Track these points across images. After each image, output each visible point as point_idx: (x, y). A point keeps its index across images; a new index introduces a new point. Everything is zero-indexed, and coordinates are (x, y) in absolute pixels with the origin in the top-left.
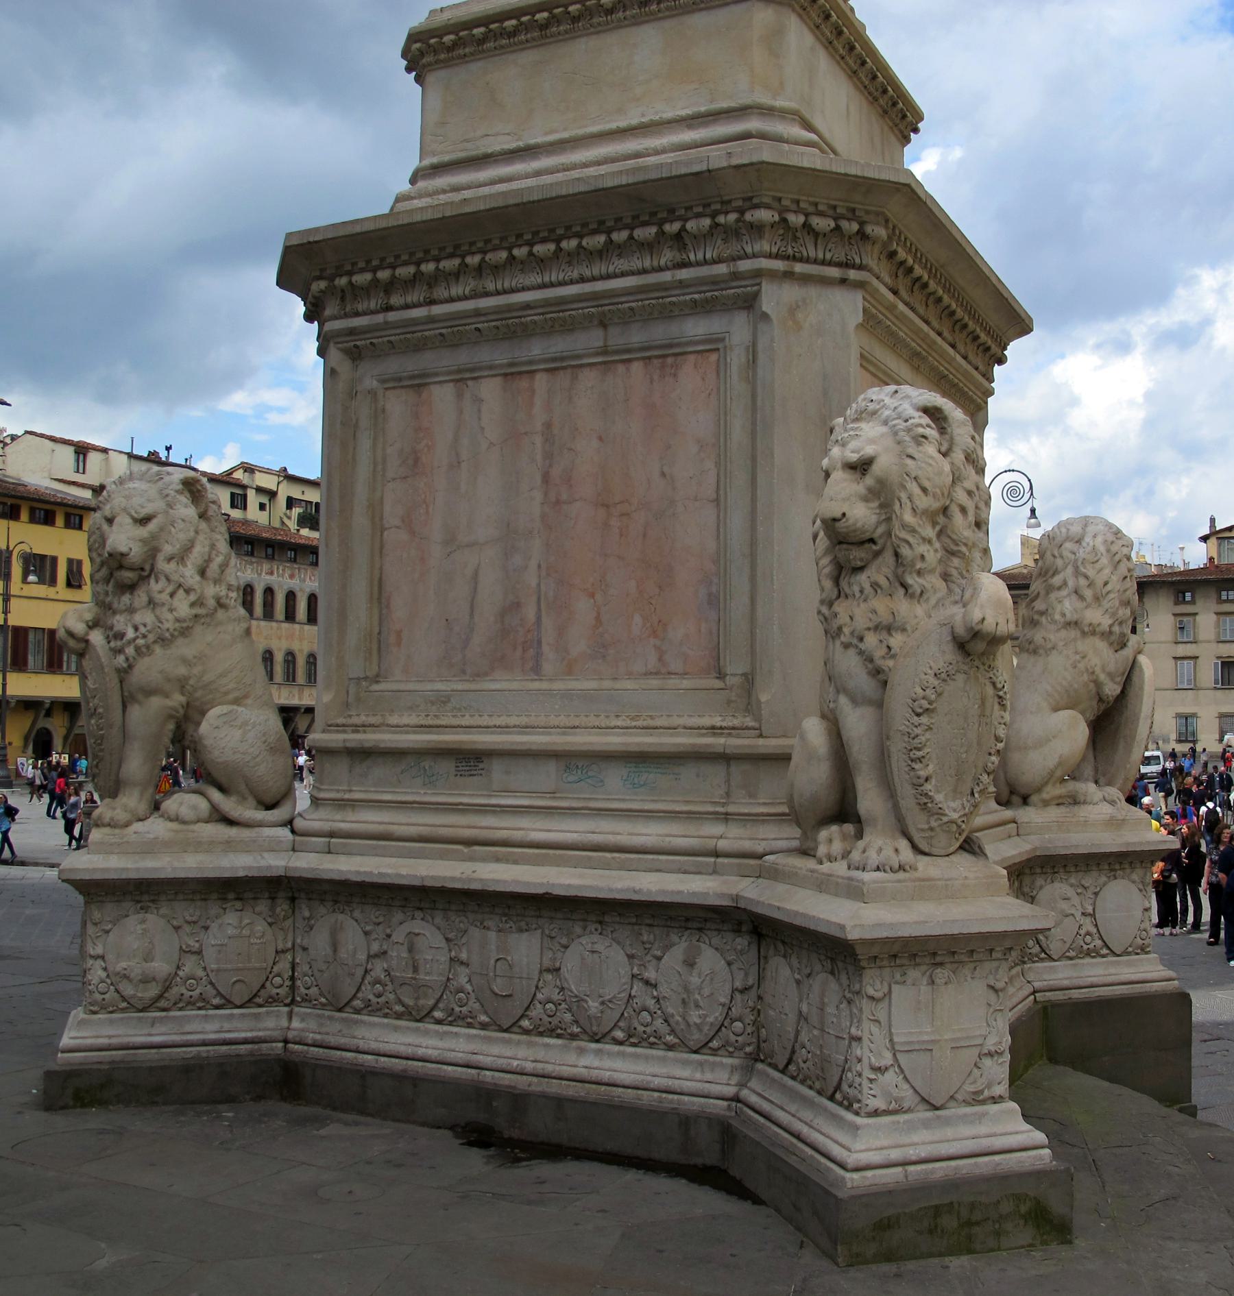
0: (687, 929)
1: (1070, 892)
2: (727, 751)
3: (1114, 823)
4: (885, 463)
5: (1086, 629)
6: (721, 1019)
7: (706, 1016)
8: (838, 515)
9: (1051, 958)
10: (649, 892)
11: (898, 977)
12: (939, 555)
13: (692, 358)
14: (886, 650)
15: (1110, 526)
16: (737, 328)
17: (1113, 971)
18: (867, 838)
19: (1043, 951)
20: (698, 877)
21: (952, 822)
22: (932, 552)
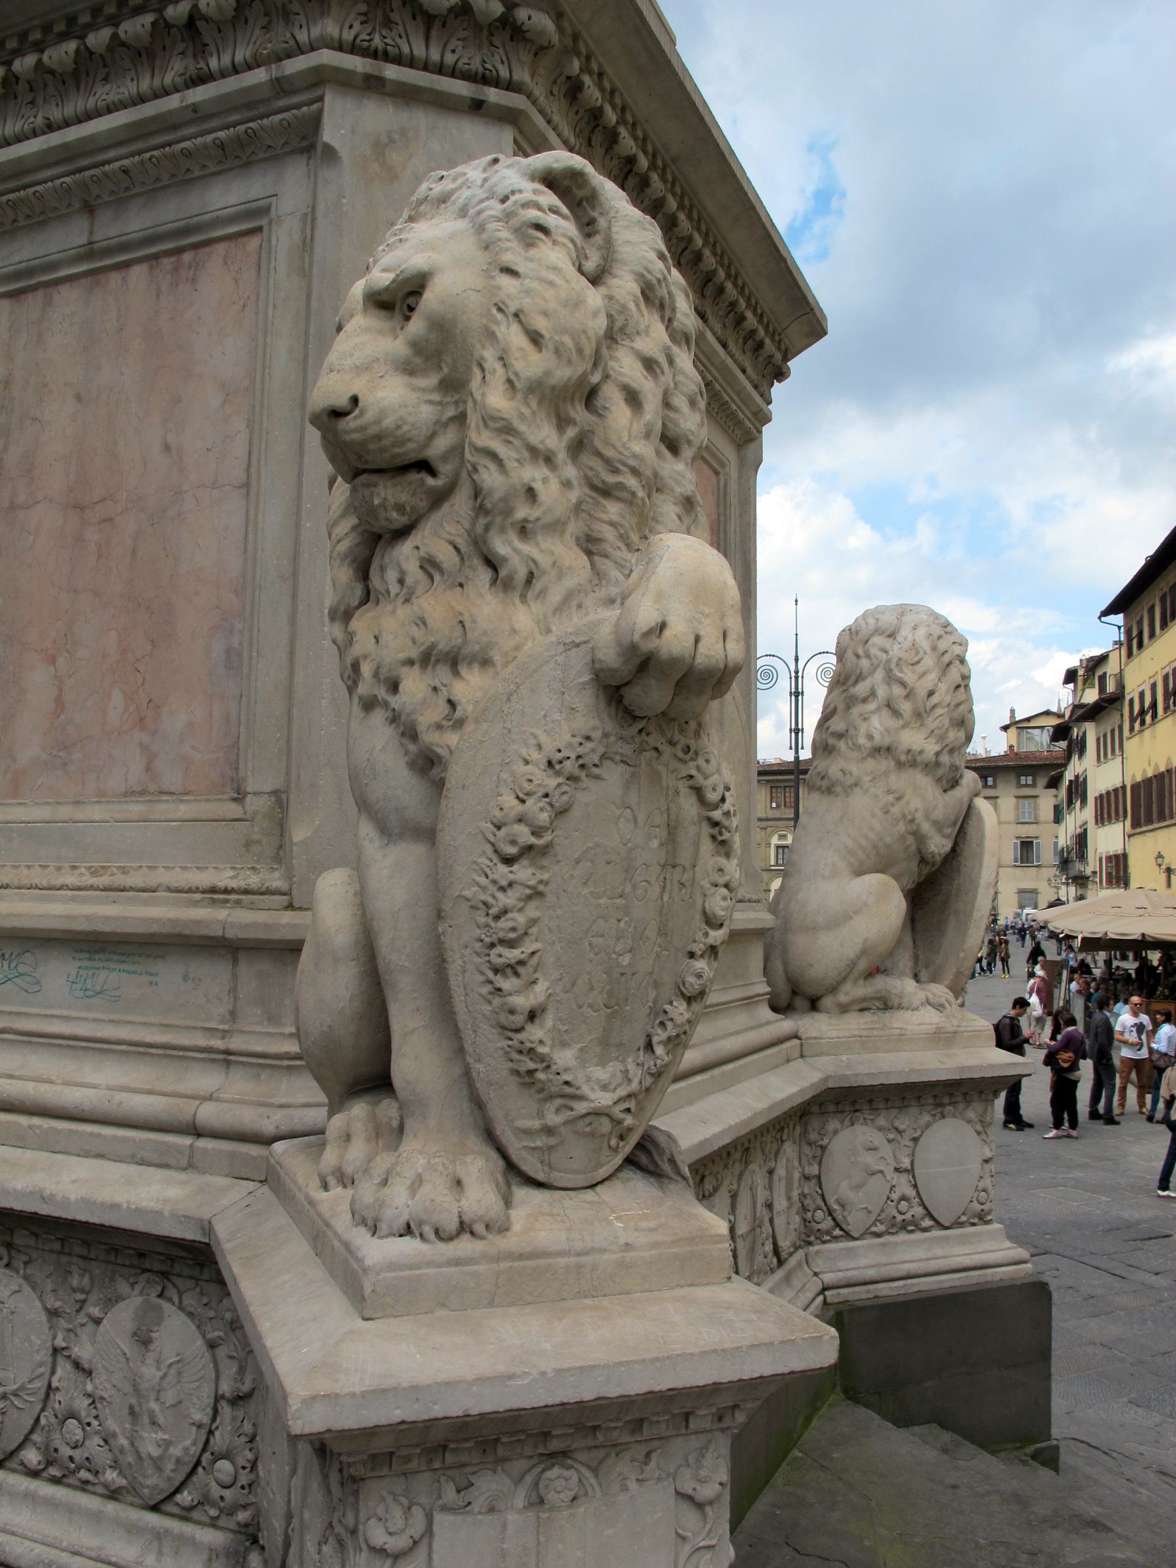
0: (145, 1271)
1: (878, 1139)
2: (230, 934)
3: (943, 1038)
4: (455, 284)
5: (903, 758)
6: (195, 1450)
7: (168, 1444)
8: (342, 401)
9: (848, 1236)
10: (66, 1202)
11: (450, 1494)
12: (574, 496)
13: (220, 248)
14: (444, 709)
15: (937, 616)
17: (939, 1252)
18: (410, 1145)
19: (838, 1225)
20: (160, 1173)
21: (597, 1113)
22: (554, 486)
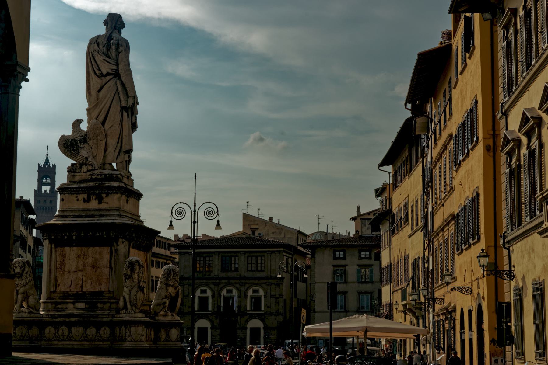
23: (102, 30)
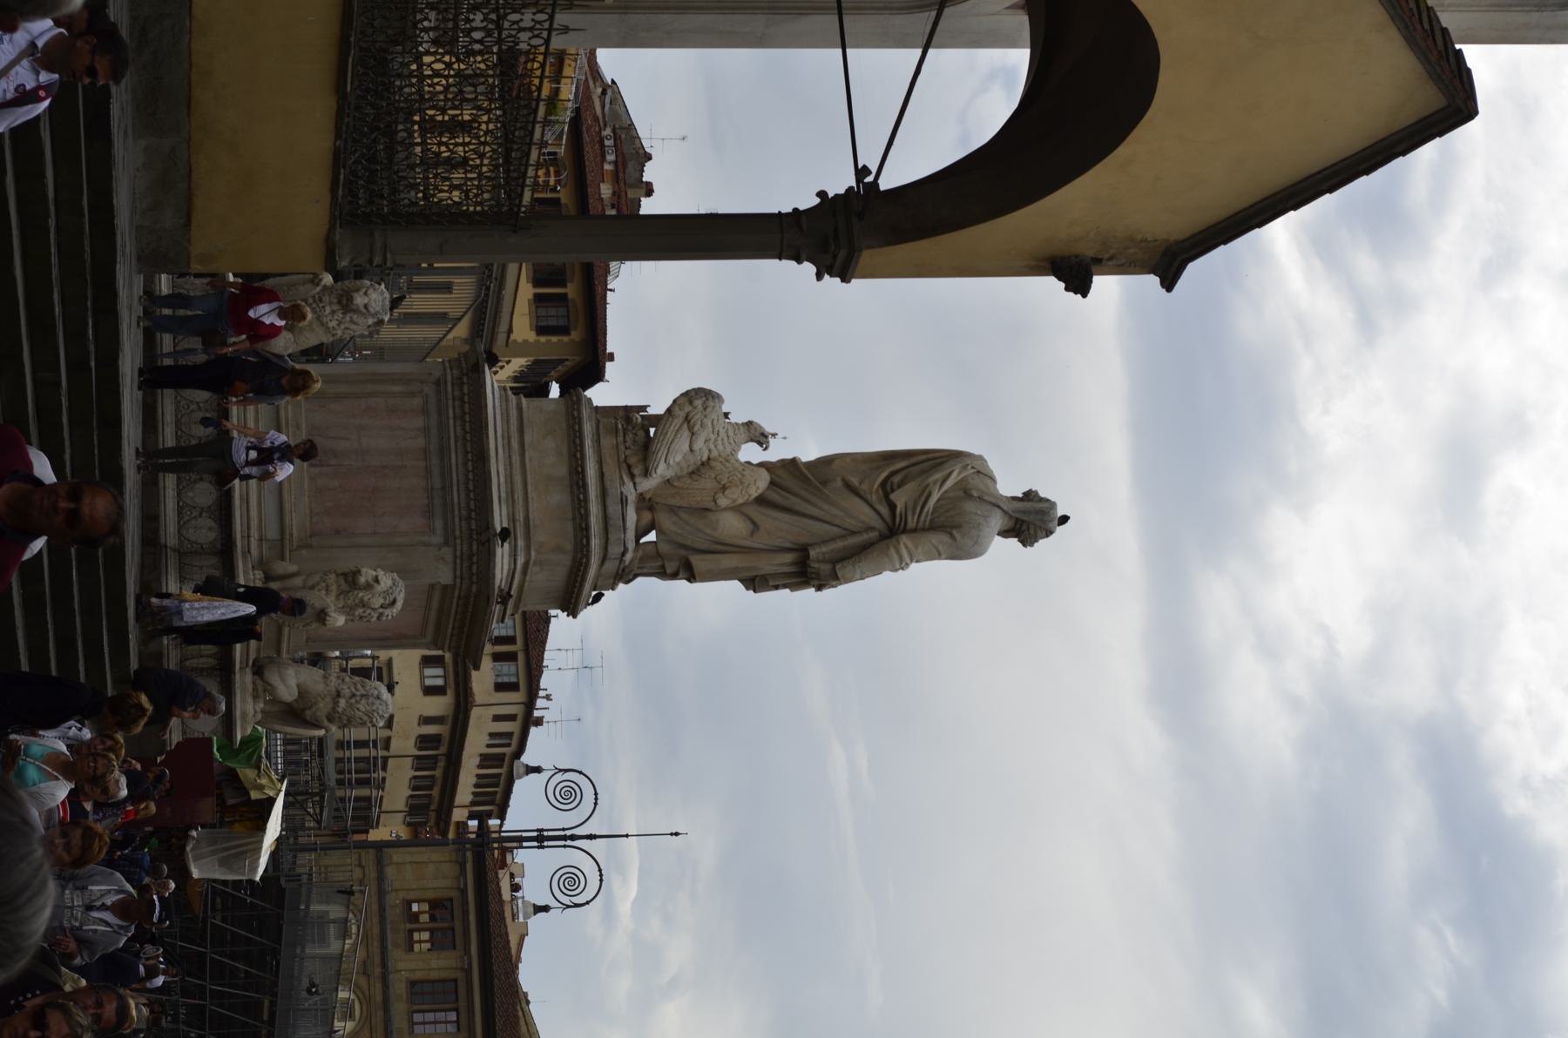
16: (438, 539)
23: (1009, 486)
